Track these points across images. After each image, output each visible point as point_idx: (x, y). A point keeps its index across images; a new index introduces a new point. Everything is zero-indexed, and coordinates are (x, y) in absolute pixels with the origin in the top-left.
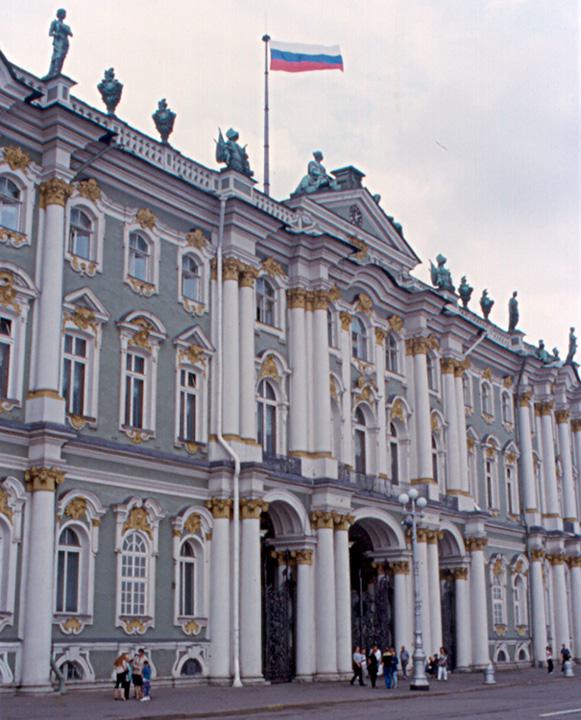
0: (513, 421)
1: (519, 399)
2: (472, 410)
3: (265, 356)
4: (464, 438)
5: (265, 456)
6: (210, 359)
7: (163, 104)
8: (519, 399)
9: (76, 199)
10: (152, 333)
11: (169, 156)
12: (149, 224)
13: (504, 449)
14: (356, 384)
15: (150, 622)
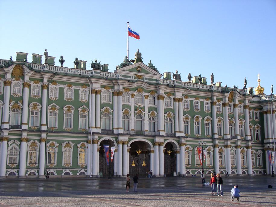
0: (210, 110)
1: (213, 104)
2: (189, 109)
3: (104, 108)
4: (182, 117)
5: (102, 130)
6: (89, 111)
7: (77, 59)
8: (213, 104)
9: (51, 86)
10: (71, 109)
11: (77, 71)
12: (71, 86)
13: (203, 119)
14: (136, 110)
15: (71, 165)
